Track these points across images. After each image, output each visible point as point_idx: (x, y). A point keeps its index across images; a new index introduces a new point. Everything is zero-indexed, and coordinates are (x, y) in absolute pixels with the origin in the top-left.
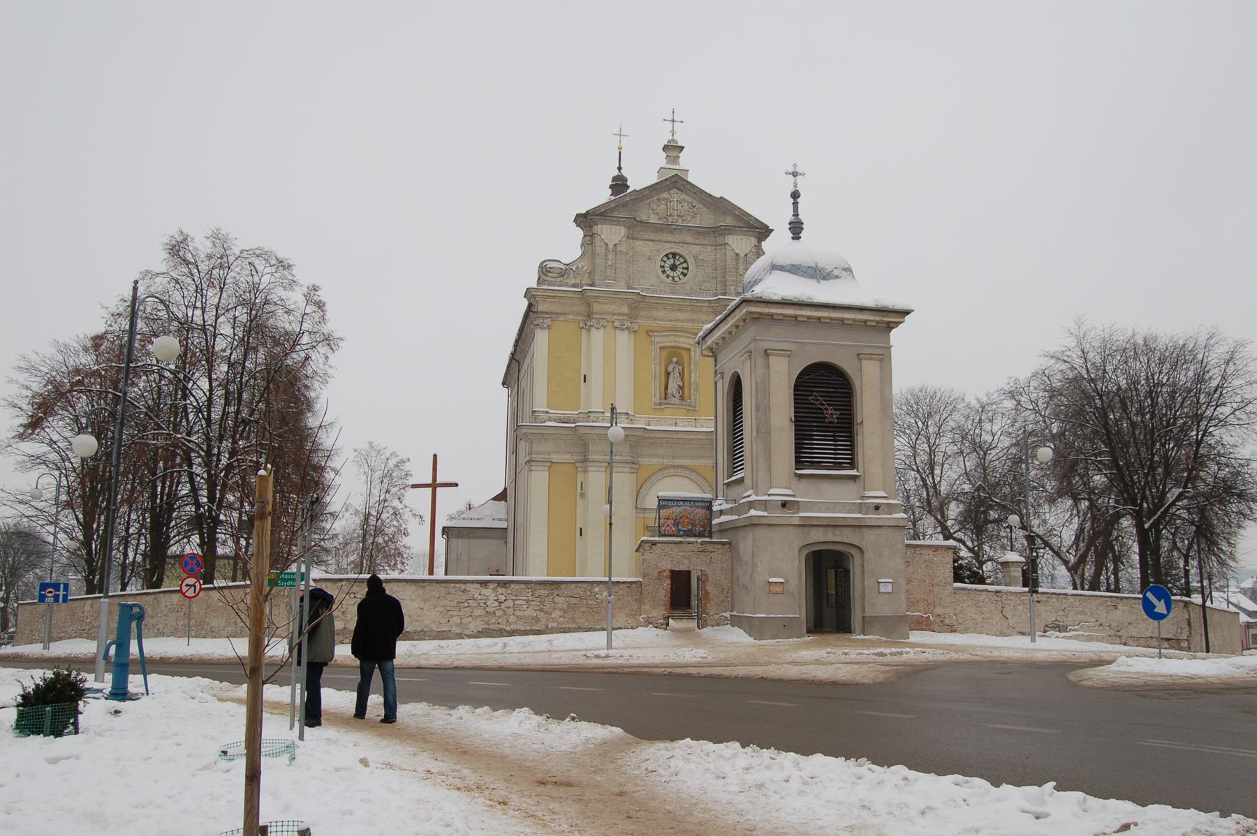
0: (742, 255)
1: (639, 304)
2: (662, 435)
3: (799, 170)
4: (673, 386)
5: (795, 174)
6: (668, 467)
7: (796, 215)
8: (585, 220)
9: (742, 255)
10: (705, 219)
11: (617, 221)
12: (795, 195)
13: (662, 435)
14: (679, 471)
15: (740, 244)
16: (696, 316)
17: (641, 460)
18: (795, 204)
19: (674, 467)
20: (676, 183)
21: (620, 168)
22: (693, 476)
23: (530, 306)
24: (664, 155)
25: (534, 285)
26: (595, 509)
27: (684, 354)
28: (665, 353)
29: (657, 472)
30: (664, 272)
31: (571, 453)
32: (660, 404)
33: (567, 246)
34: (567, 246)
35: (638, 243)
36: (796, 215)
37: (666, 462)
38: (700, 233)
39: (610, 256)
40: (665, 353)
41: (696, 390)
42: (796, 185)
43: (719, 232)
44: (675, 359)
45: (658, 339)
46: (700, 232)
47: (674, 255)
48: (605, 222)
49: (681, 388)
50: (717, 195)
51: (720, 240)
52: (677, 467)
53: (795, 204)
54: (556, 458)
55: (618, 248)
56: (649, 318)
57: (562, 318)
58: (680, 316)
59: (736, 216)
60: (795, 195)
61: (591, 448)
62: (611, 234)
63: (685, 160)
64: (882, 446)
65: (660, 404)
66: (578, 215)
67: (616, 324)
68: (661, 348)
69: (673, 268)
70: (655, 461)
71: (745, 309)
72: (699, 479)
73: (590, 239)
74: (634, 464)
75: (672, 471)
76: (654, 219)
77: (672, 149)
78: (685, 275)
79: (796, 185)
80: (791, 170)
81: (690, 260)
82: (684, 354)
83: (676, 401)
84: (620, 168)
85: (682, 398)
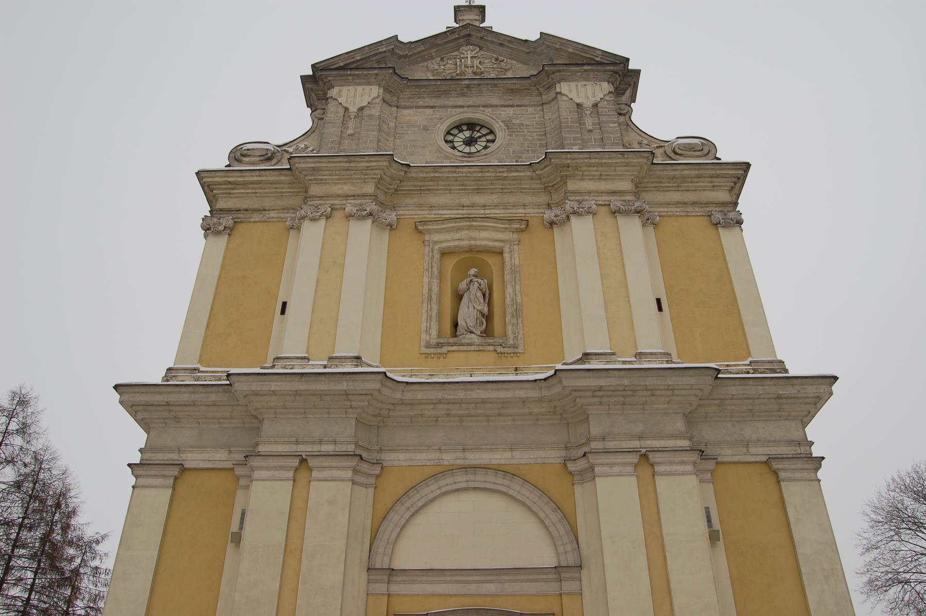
2: (434, 394)
6: (451, 470)
13: (434, 394)
14: (480, 479)
16: (511, 199)
17: (389, 458)
19: (466, 468)
22: (515, 487)
27: (492, 261)
28: (450, 263)
29: (425, 481)
32: (439, 345)
33: (286, 120)
34: (286, 120)
35: (405, 112)
37: (448, 458)
39: (351, 124)
40: (450, 263)
41: (517, 313)
44: (473, 271)
45: (436, 237)
47: (471, 126)
50: (534, 36)
52: (475, 468)
54: (193, 459)
55: (366, 112)
56: (420, 206)
57: (257, 217)
58: (479, 199)
61: (268, 428)
62: (352, 96)
65: (439, 345)
68: (444, 254)
69: (470, 142)
70: (422, 457)
72: (528, 494)
74: (364, 461)
75: (461, 479)
81: (498, 127)
82: (492, 261)
85: (488, 332)
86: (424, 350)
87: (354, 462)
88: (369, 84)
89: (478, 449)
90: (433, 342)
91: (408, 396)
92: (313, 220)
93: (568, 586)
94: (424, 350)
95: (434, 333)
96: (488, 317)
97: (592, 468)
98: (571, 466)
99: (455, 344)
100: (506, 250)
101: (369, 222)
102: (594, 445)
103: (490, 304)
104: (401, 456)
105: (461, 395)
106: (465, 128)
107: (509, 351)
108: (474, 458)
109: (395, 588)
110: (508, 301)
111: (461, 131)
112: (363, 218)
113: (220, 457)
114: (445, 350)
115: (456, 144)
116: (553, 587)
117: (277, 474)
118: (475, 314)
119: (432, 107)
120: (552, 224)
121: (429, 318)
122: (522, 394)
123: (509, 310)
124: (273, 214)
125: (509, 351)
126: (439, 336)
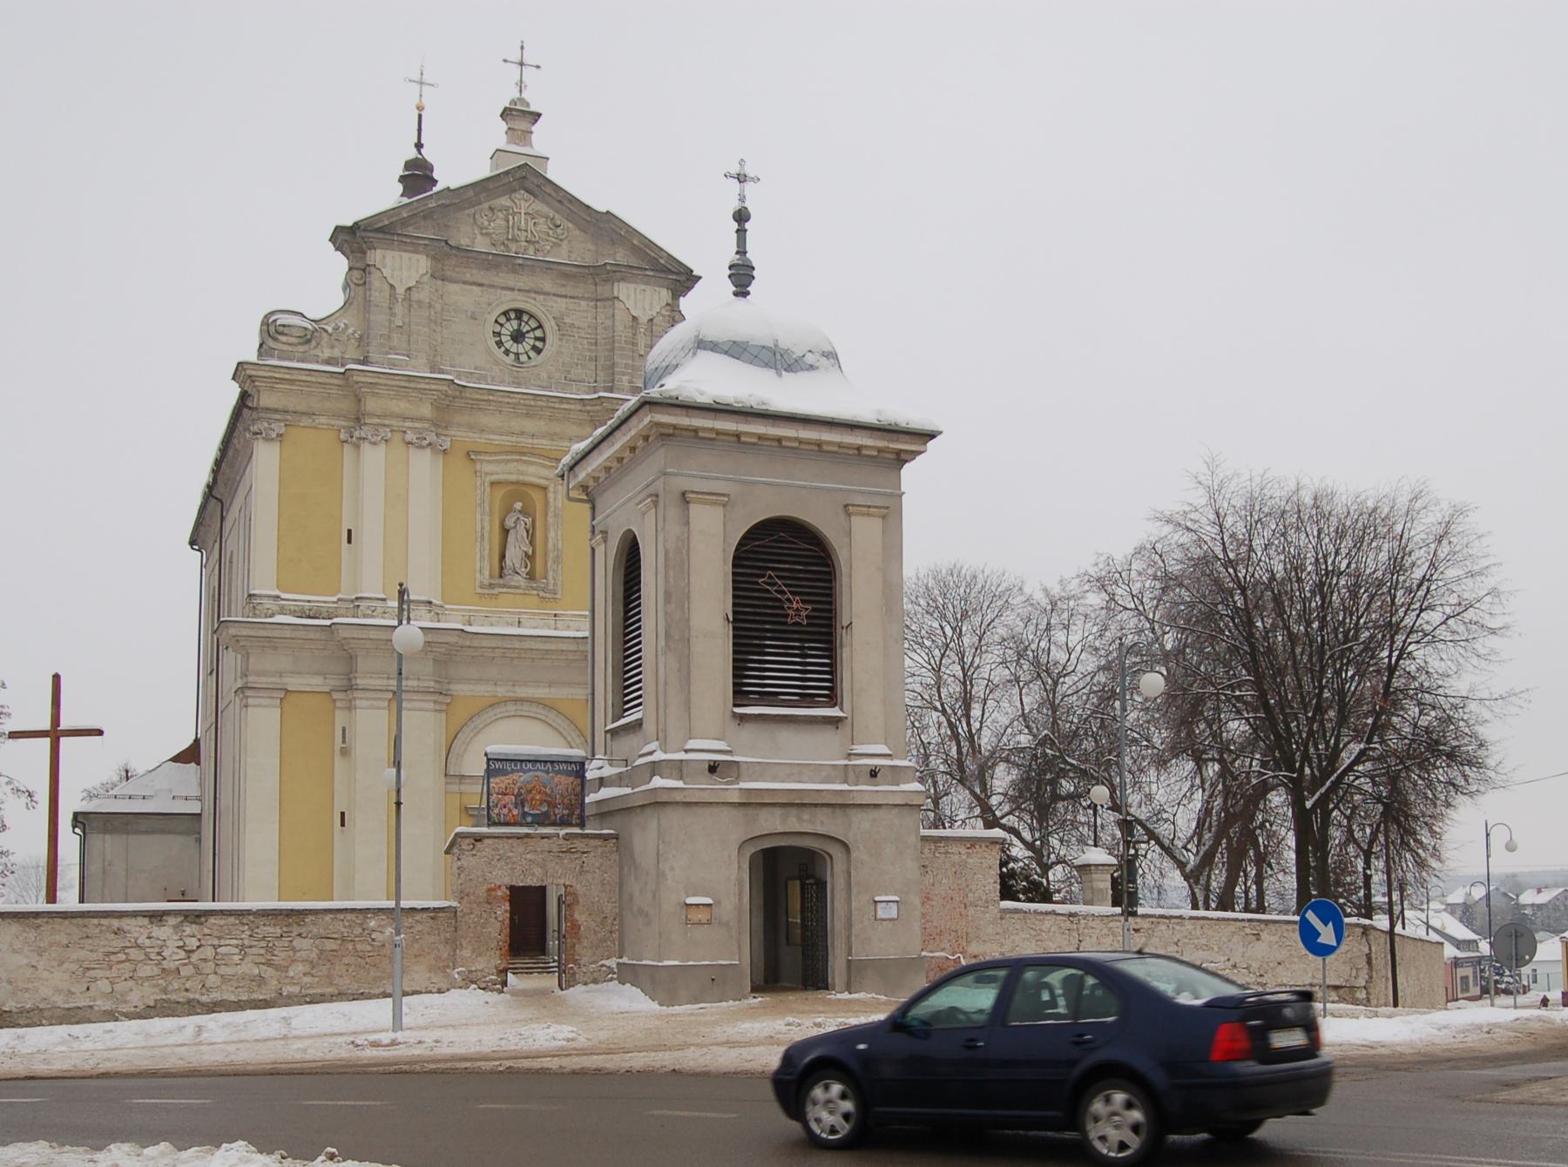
0: (644, 319)
1: (452, 402)
2: (494, 643)
3: (750, 171)
4: (514, 555)
5: (741, 178)
7: (742, 251)
8: (351, 239)
9: (644, 319)
10: (577, 250)
11: (413, 245)
12: (741, 217)
13: (494, 643)
15: (639, 299)
16: (557, 428)
18: (741, 232)
20: (523, 179)
21: (419, 146)
22: (552, 717)
23: (244, 396)
24: (503, 126)
25: (252, 357)
26: (368, 777)
27: (536, 496)
28: (500, 493)
30: (500, 344)
31: (324, 675)
32: (491, 586)
34: (319, 287)
35: (453, 287)
36: (742, 251)
37: (502, 691)
38: (566, 276)
39: (399, 309)
40: (500, 493)
41: (557, 560)
42: (742, 199)
43: (601, 275)
44: (518, 505)
45: (487, 468)
47: (519, 313)
48: (390, 246)
49: (530, 557)
50: (600, 206)
51: (603, 290)
53: (741, 232)
54: (293, 683)
55: (415, 296)
56: (471, 428)
57: (305, 421)
58: (530, 425)
59: (635, 250)
60: (741, 217)
61: (363, 664)
62: (401, 268)
63: (542, 139)
64: (883, 665)
65: (491, 586)
66: (339, 230)
67: (410, 436)
68: (492, 484)
69: (518, 337)
70: (482, 689)
71: (647, 418)
72: (559, 722)
73: (360, 276)
74: (441, 695)
75: (511, 708)
76: (482, 245)
77: (520, 116)
78: (539, 351)
79: (742, 199)
80: (735, 170)
81: (549, 325)
83: (520, 581)
84: (419, 146)
85: (531, 576)
86: (479, 590)
88: (416, 252)
89: (525, 684)
90: (486, 582)
91: (476, 643)
92: (374, 444)
94: (479, 590)
95: (487, 573)
96: (530, 557)
99: (504, 586)
100: (551, 489)
101: (429, 451)
103: (532, 543)
104: (466, 687)
105: (517, 645)
106: (513, 315)
108: (522, 692)
110: (550, 545)
111: (508, 320)
112: (421, 447)
113: (316, 682)
114: (496, 591)
115: (504, 339)
117: (375, 703)
118: (520, 554)
119: (481, 285)
121: (482, 557)
122: (563, 647)
123: (551, 555)
124: (323, 420)
126: (491, 576)
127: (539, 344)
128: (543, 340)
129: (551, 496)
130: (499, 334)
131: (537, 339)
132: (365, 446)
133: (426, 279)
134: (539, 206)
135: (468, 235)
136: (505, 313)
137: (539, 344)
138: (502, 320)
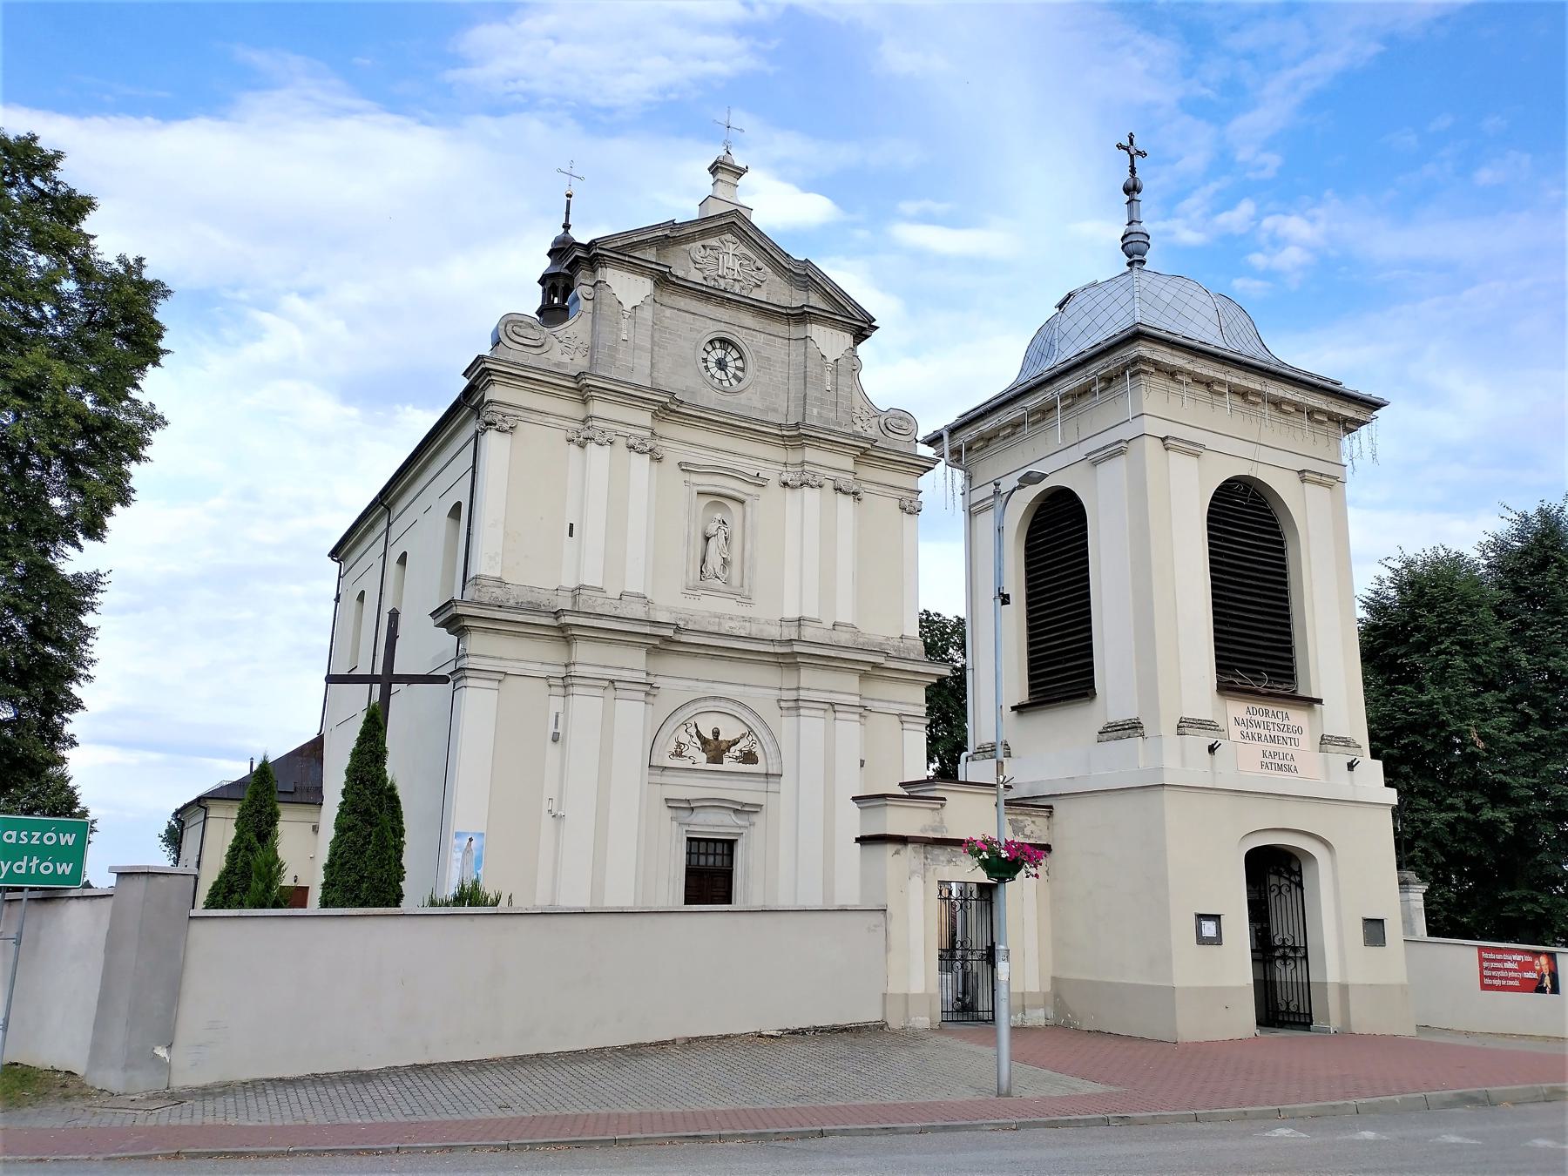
0: (831, 359)
1: (668, 409)
4: (714, 561)
9: (831, 359)
11: (638, 268)
15: (829, 341)
35: (668, 312)
46: (763, 311)
47: (725, 343)
51: (796, 331)
67: (631, 442)
76: (696, 276)
78: (740, 380)
87: (647, 688)
93: (772, 787)
97: (798, 708)
98: (783, 704)
102: (803, 694)
106: (718, 345)
107: (746, 600)
109: (665, 780)
112: (642, 453)
116: (763, 786)
120: (786, 484)
125: (746, 600)
127: (739, 374)
128: (742, 370)
129: (748, 509)
130: (705, 360)
131: (737, 368)
132: (591, 446)
133: (649, 300)
134: (743, 249)
135: (684, 264)
136: (711, 342)
137: (739, 374)
138: (709, 348)
